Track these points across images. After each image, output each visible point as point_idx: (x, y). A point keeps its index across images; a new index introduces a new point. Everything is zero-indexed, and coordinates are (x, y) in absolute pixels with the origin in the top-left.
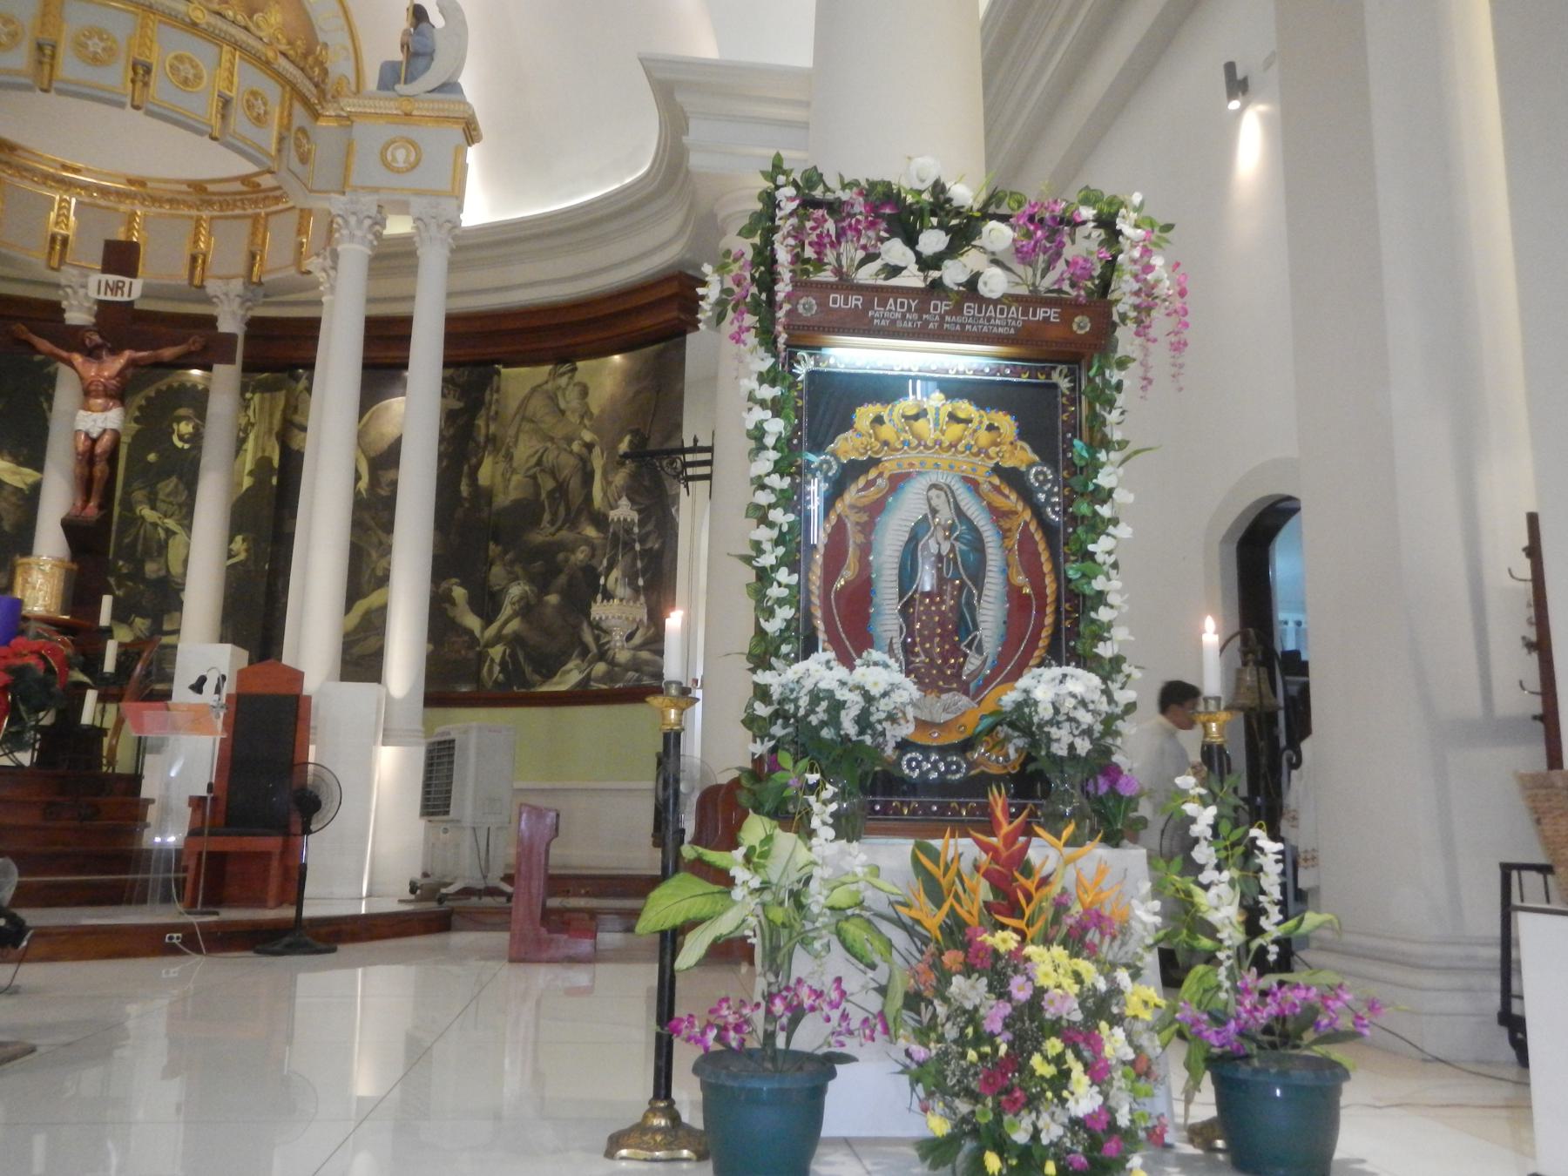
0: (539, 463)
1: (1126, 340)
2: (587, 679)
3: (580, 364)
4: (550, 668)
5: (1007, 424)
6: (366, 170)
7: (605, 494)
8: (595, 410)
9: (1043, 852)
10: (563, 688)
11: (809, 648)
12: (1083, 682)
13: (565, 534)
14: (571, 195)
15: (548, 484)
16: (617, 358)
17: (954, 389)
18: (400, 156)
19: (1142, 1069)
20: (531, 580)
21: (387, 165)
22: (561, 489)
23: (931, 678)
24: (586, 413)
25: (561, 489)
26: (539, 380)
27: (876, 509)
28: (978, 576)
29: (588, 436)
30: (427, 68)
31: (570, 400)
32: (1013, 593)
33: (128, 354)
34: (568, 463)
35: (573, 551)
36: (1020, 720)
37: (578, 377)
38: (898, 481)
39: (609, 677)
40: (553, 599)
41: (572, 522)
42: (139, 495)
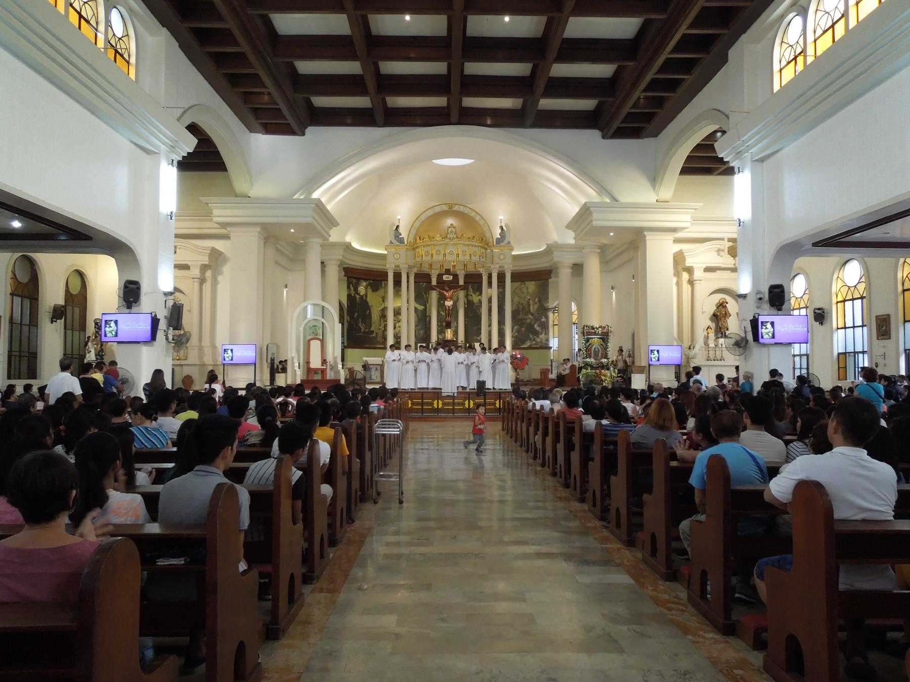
0: (519, 302)
1: (610, 334)
2: (531, 345)
3: (526, 283)
4: (524, 343)
5: (601, 340)
6: (496, 259)
7: (533, 308)
8: (530, 292)
9: (602, 371)
10: (526, 346)
11: (587, 358)
12: (606, 360)
13: (525, 317)
14: (525, 251)
15: (521, 307)
16: (533, 282)
17: (597, 338)
18: (502, 257)
19: (608, 383)
20: (518, 325)
21: (500, 259)
22: (523, 309)
23: (595, 360)
24: (528, 293)
25: (523, 309)
26: (517, 286)
27: (592, 347)
28: (599, 351)
29: (529, 298)
30: (504, 240)
31: (524, 290)
32: (602, 353)
33: (452, 291)
34: (525, 302)
35: (527, 320)
36: (602, 362)
37: (526, 285)
38: (593, 345)
39: (536, 344)
40: (523, 329)
41: (526, 314)
42: (440, 310)
